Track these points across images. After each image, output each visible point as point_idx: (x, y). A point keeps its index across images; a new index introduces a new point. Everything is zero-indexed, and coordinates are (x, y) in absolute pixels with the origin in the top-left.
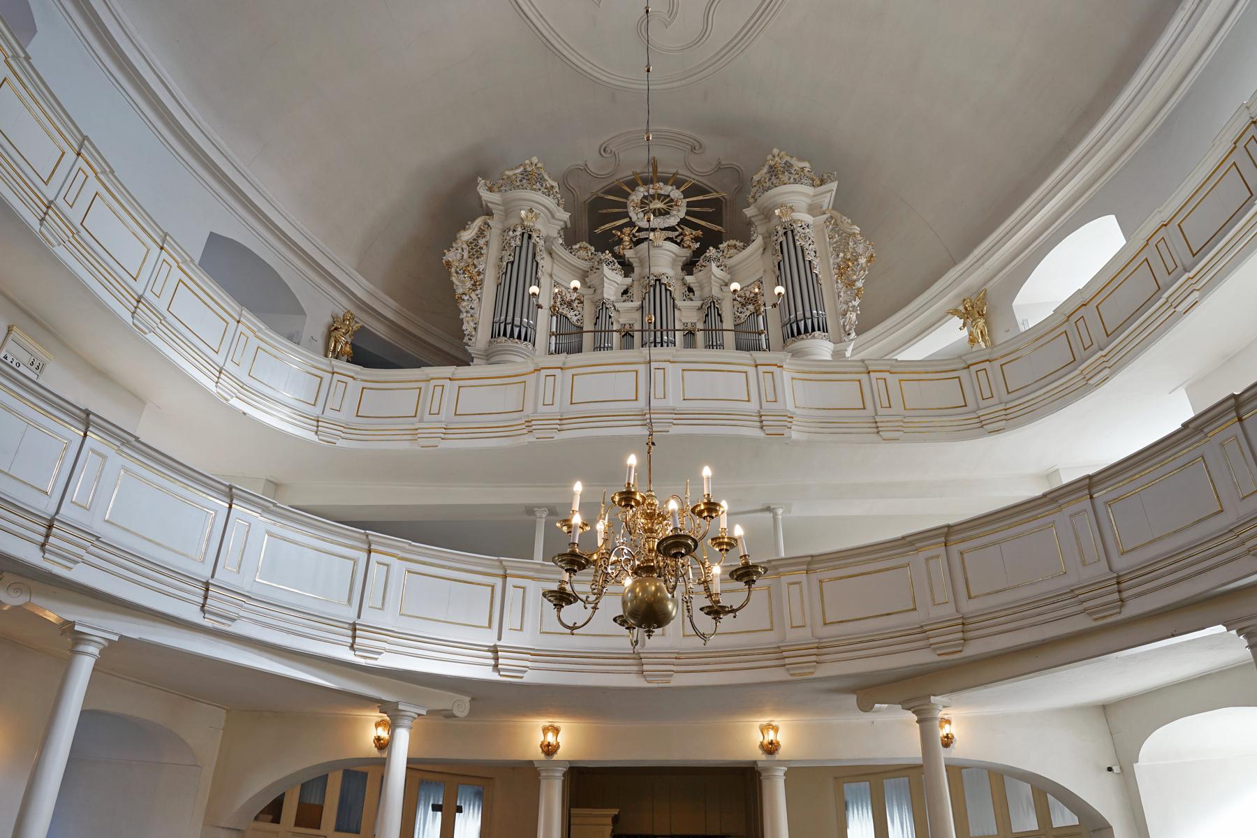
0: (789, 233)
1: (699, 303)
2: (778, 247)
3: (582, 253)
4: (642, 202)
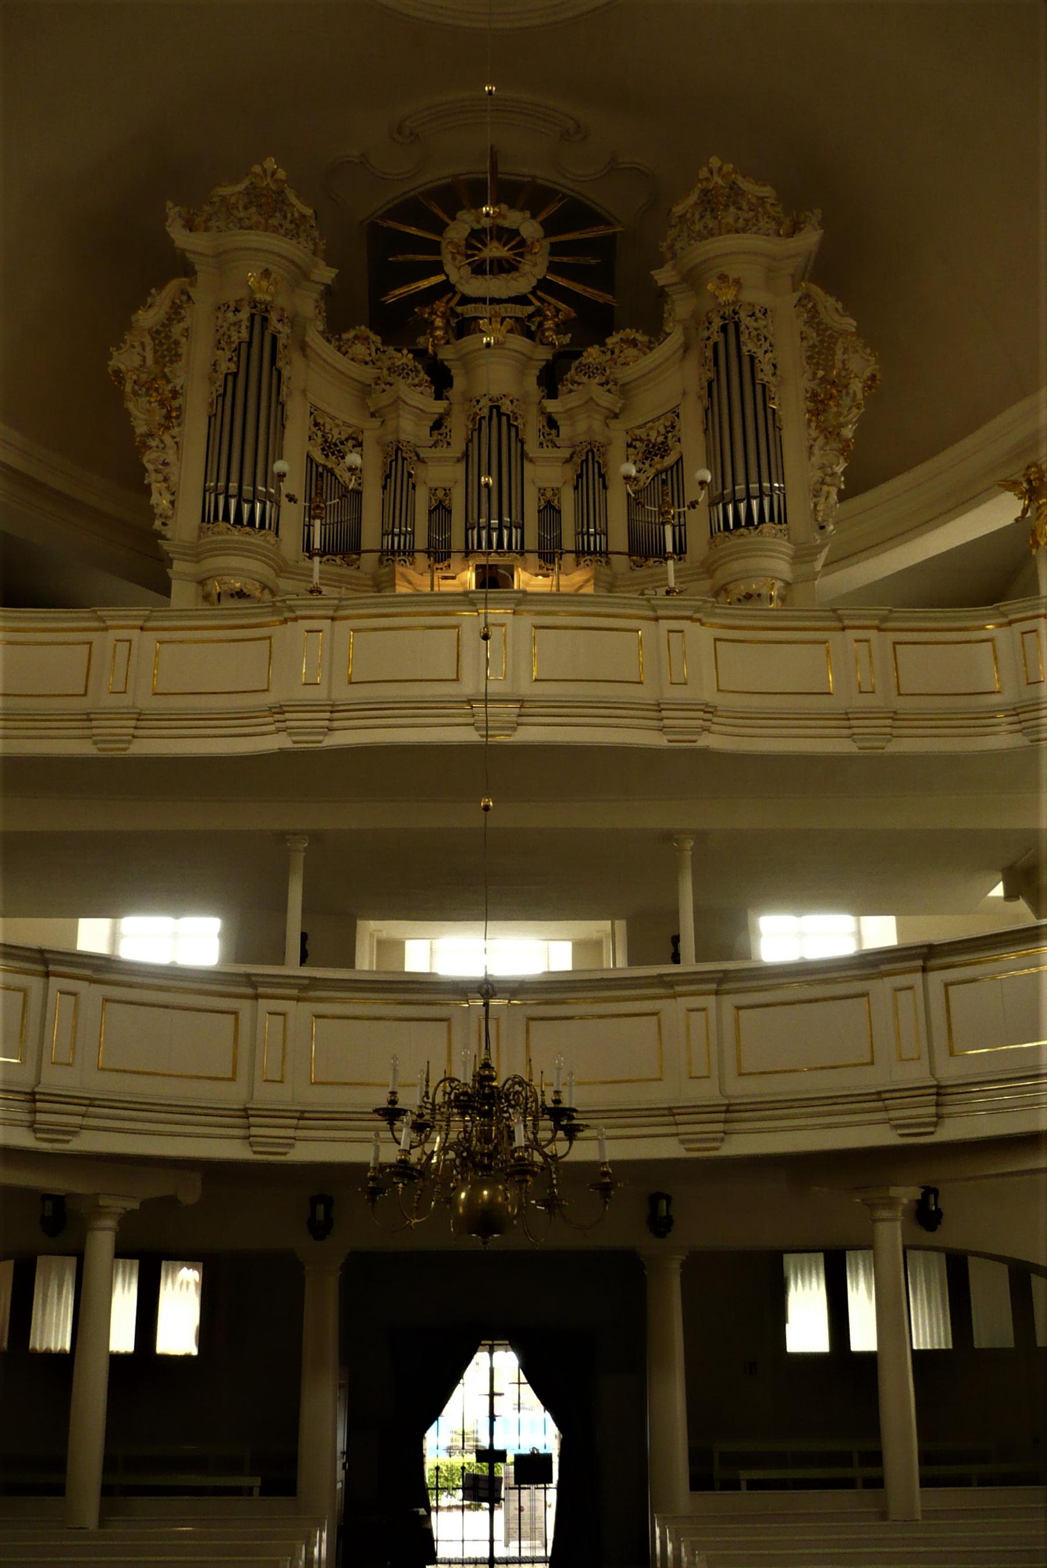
0: (731, 329)
1: (566, 453)
2: (709, 353)
4: (469, 246)
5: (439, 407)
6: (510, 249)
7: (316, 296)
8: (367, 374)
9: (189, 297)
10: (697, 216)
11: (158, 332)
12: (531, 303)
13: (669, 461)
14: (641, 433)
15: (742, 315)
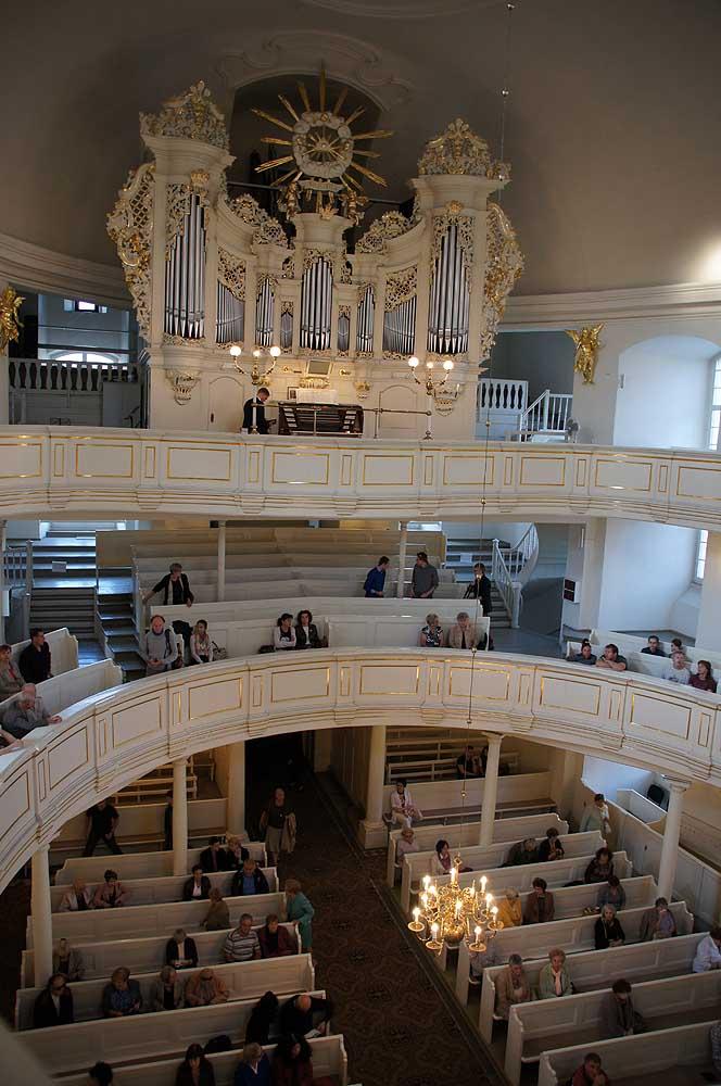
3: (245, 210)
5: (289, 253)
6: (333, 146)
7: (221, 171)
8: (250, 229)
9: (152, 178)
10: (443, 154)
11: (135, 202)
12: (340, 183)
13: (409, 297)
14: (395, 277)
15: (460, 223)
